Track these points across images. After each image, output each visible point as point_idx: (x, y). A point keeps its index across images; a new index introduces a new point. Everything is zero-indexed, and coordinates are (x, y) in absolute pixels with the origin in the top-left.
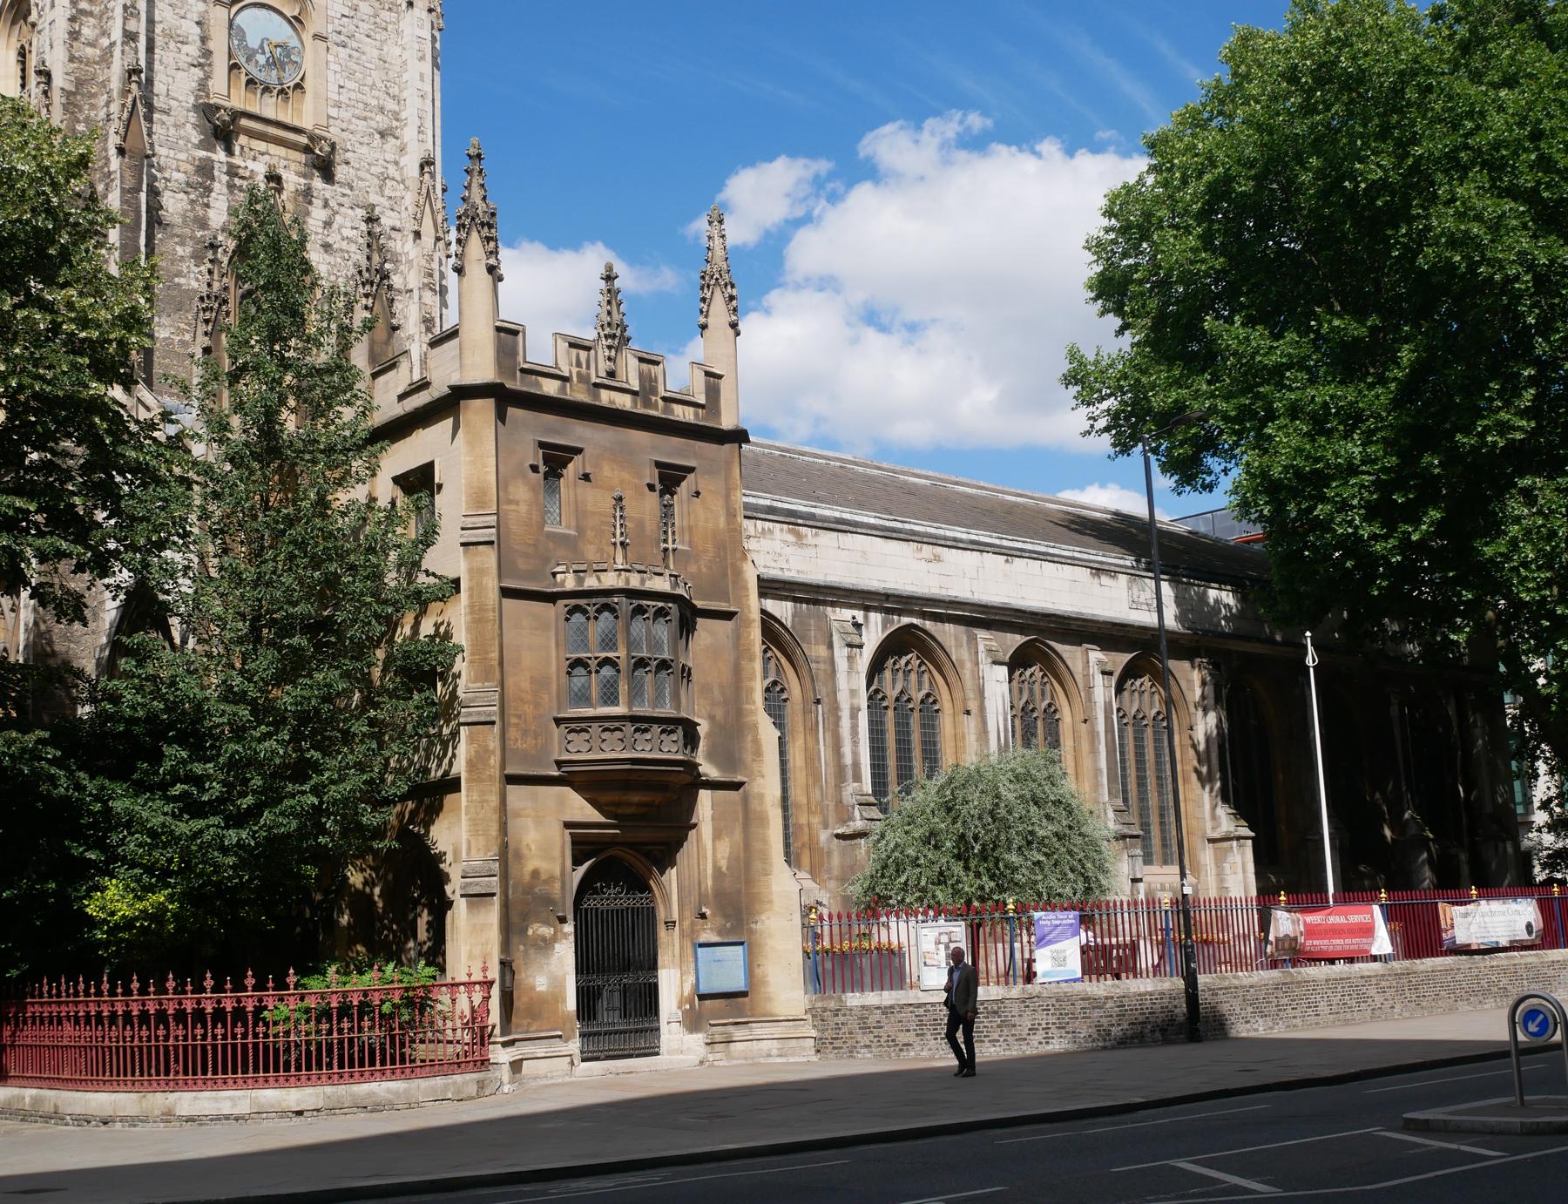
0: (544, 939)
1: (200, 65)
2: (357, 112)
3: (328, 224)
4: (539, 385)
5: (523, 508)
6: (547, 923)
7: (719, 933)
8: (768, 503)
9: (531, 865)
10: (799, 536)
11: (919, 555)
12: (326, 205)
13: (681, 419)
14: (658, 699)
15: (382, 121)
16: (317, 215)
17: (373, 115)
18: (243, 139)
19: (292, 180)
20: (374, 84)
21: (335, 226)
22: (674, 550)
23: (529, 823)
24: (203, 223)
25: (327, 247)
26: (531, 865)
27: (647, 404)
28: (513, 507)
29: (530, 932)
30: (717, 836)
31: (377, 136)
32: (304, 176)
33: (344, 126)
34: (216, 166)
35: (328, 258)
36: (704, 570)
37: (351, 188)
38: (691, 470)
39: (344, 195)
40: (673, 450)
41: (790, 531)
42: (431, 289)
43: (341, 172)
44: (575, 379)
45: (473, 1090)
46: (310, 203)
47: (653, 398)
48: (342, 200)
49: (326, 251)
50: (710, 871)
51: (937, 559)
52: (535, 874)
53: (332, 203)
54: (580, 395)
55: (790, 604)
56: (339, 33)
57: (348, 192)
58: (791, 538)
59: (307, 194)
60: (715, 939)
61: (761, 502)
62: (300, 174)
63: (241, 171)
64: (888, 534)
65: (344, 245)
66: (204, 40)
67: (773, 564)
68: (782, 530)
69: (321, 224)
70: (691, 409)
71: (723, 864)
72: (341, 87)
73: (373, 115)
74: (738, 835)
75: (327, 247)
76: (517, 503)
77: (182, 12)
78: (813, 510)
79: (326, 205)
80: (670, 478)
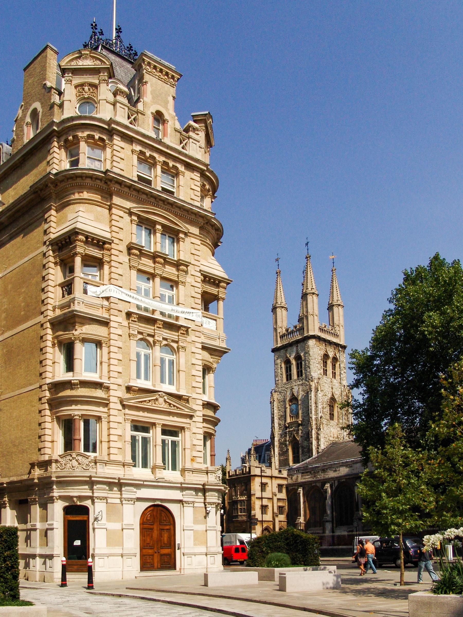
24: (286, 441)
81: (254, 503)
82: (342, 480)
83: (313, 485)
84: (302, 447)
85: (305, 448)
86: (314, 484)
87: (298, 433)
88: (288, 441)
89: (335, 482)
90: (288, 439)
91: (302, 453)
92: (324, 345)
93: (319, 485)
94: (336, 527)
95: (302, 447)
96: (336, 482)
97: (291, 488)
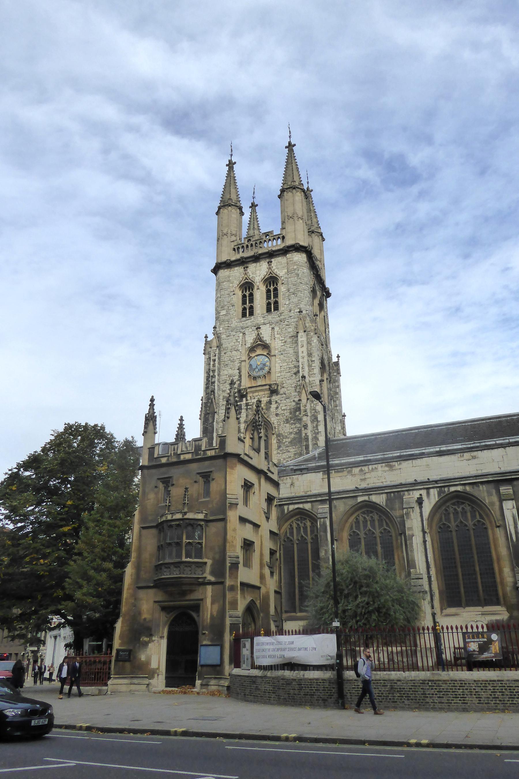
0: (145, 642)
1: (239, 380)
2: (287, 371)
3: (277, 408)
4: (161, 461)
5: (152, 500)
6: (147, 637)
7: (211, 641)
8: (398, 454)
9: (143, 617)
10: (391, 467)
11: (462, 459)
12: (276, 402)
13: (210, 455)
14: (164, 558)
15: (295, 370)
16: (274, 406)
17: (292, 370)
18: (251, 395)
19: (265, 400)
20: (292, 360)
21: (280, 407)
22: (188, 503)
23: (144, 602)
25: (277, 415)
26: (143, 617)
27: (197, 454)
28: (149, 501)
29: (141, 640)
30: (213, 603)
31: (294, 375)
32: (269, 397)
33: (283, 377)
34: (242, 405)
35: (277, 418)
36: (214, 505)
37: (285, 394)
38: (211, 472)
39: (282, 397)
40: (204, 467)
41: (386, 466)
42: (306, 415)
43: (282, 391)
44: (172, 455)
45: (97, 692)
46: (271, 404)
47: (200, 452)
48: (282, 399)
49: (277, 416)
50: (209, 617)
51: (474, 458)
52: (145, 619)
53: (279, 401)
54: (174, 460)
55: (384, 496)
56: (281, 351)
57: (284, 395)
58: (387, 469)
59: (270, 402)
60: (209, 643)
61: (395, 455)
62: (268, 397)
63: (250, 404)
64: (441, 454)
65: (282, 412)
66: (240, 373)
67: (378, 481)
68: (382, 467)
69: (275, 409)
70: (214, 451)
71: (215, 614)
72: (281, 366)
73: (292, 370)
74: (221, 602)
75: (277, 415)
76: (150, 499)
77: (234, 369)
78: (424, 451)
79: (276, 402)
80: (207, 477)
81: (234, 530)
82: (452, 489)
83: (360, 499)
84: (278, 435)
85: (286, 437)
86: (366, 498)
87: (270, 407)
88: (245, 422)
89: (428, 494)
90: (242, 420)
91: (279, 447)
92: (312, 273)
93: (379, 499)
94: (442, 609)
95: (278, 435)
96: (434, 492)
97: (291, 507)
